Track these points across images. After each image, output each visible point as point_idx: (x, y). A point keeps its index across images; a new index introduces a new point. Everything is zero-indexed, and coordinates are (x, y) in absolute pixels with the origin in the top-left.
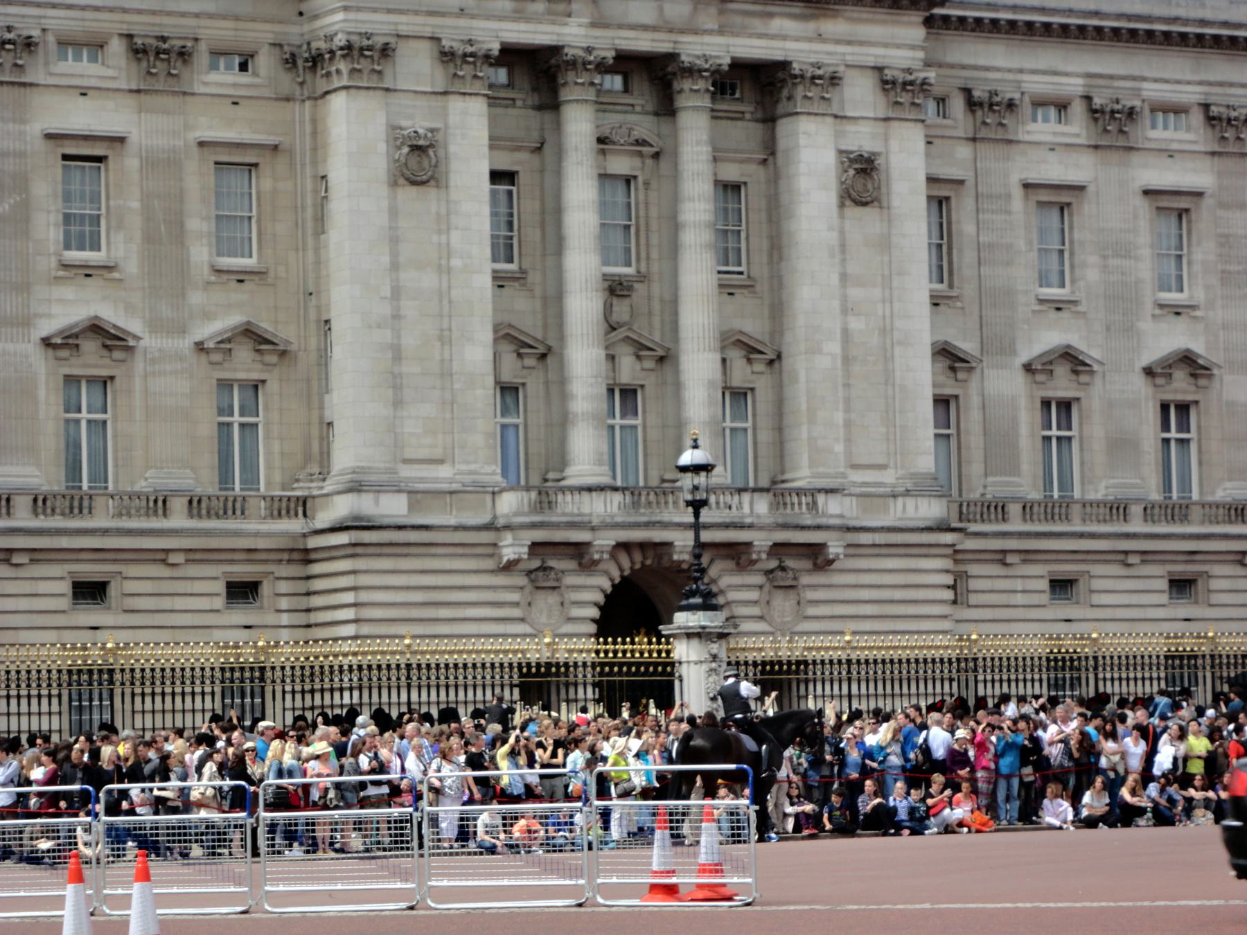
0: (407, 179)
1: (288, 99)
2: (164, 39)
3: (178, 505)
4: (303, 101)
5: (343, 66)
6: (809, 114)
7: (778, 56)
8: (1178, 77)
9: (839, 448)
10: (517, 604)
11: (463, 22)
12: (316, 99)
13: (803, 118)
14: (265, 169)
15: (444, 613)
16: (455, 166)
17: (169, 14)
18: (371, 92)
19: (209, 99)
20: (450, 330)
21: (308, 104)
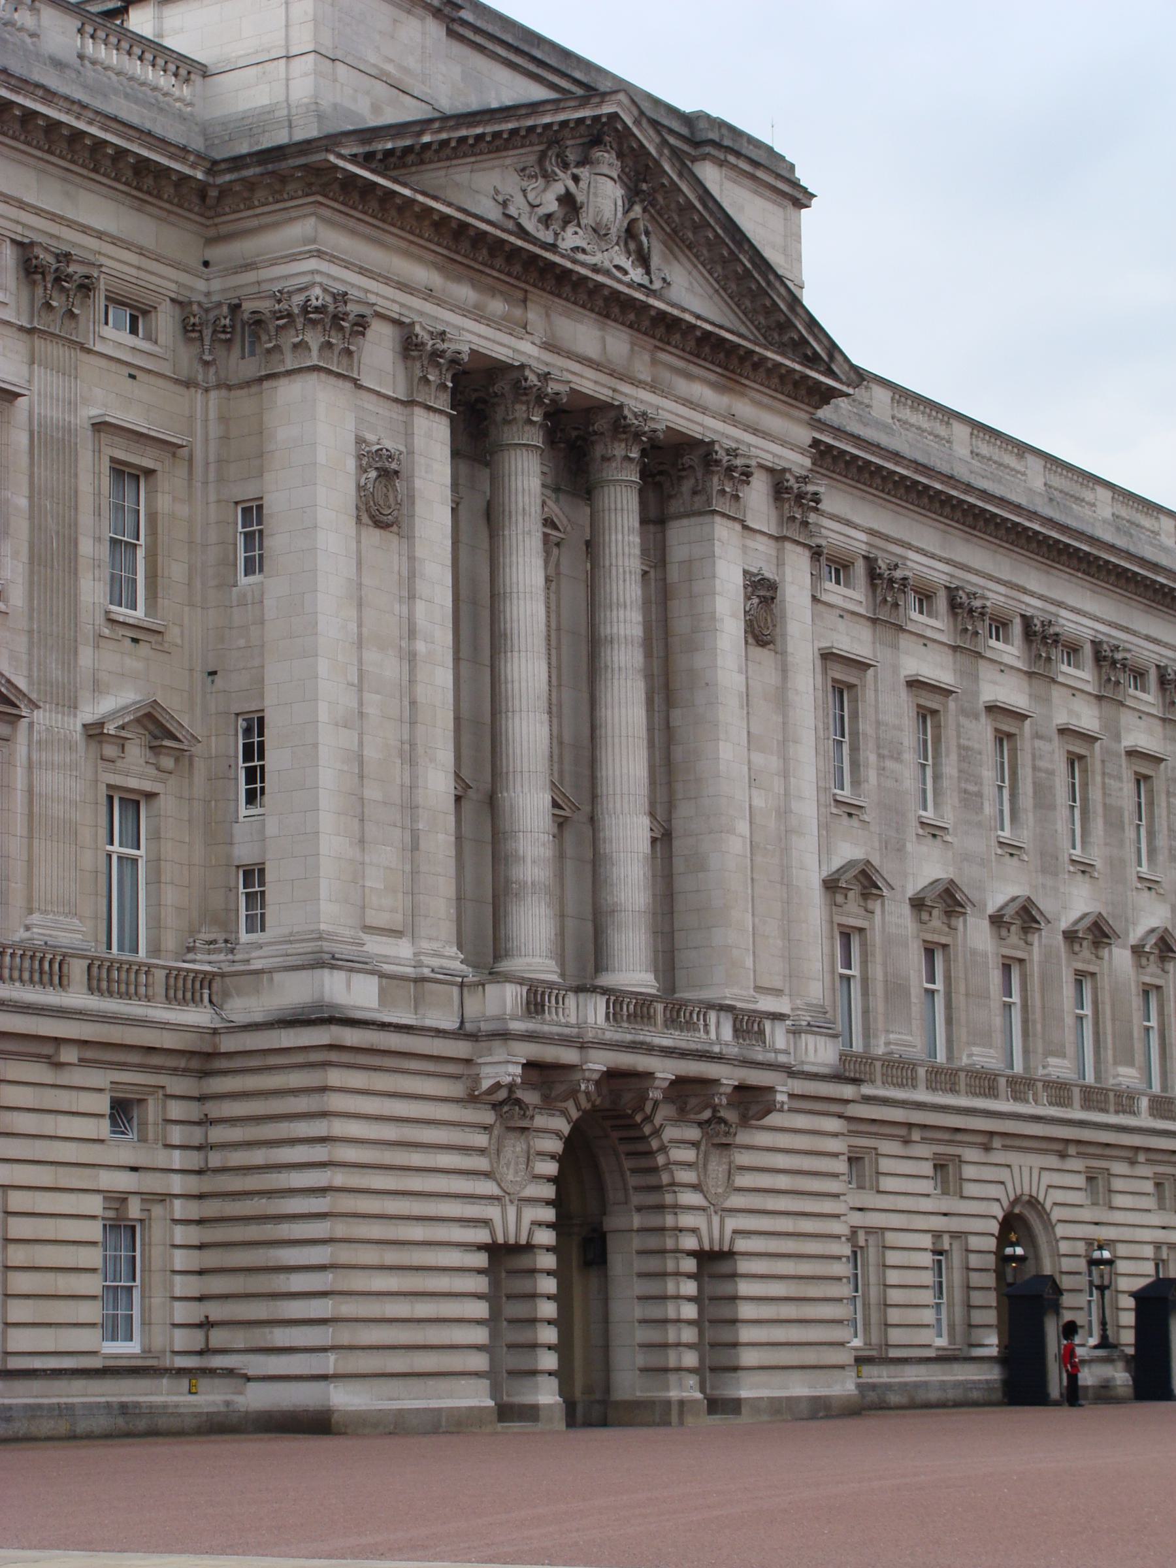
0: (372, 517)
1: (188, 384)
2: (67, 257)
3: (77, 969)
4: (207, 390)
5: (314, 338)
6: (724, 515)
7: (696, 432)
8: (931, 549)
9: (749, 963)
10: (482, 1151)
11: (429, 308)
12: (229, 388)
13: (718, 519)
14: (163, 481)
15: (417, 1159)
16: (420, 508)
17: (71, 224)
18: (340, 383)
19: (103, 363)
20: (413, 745)
21: (213, 394)
